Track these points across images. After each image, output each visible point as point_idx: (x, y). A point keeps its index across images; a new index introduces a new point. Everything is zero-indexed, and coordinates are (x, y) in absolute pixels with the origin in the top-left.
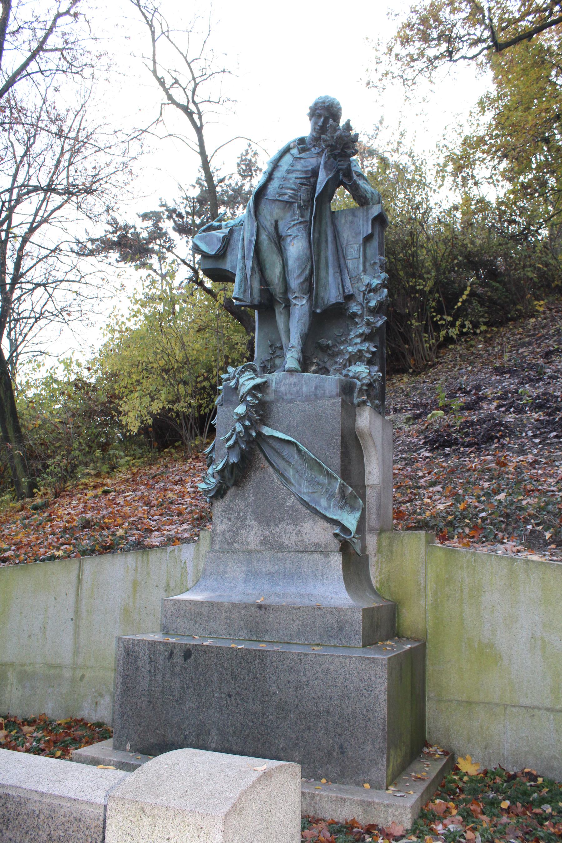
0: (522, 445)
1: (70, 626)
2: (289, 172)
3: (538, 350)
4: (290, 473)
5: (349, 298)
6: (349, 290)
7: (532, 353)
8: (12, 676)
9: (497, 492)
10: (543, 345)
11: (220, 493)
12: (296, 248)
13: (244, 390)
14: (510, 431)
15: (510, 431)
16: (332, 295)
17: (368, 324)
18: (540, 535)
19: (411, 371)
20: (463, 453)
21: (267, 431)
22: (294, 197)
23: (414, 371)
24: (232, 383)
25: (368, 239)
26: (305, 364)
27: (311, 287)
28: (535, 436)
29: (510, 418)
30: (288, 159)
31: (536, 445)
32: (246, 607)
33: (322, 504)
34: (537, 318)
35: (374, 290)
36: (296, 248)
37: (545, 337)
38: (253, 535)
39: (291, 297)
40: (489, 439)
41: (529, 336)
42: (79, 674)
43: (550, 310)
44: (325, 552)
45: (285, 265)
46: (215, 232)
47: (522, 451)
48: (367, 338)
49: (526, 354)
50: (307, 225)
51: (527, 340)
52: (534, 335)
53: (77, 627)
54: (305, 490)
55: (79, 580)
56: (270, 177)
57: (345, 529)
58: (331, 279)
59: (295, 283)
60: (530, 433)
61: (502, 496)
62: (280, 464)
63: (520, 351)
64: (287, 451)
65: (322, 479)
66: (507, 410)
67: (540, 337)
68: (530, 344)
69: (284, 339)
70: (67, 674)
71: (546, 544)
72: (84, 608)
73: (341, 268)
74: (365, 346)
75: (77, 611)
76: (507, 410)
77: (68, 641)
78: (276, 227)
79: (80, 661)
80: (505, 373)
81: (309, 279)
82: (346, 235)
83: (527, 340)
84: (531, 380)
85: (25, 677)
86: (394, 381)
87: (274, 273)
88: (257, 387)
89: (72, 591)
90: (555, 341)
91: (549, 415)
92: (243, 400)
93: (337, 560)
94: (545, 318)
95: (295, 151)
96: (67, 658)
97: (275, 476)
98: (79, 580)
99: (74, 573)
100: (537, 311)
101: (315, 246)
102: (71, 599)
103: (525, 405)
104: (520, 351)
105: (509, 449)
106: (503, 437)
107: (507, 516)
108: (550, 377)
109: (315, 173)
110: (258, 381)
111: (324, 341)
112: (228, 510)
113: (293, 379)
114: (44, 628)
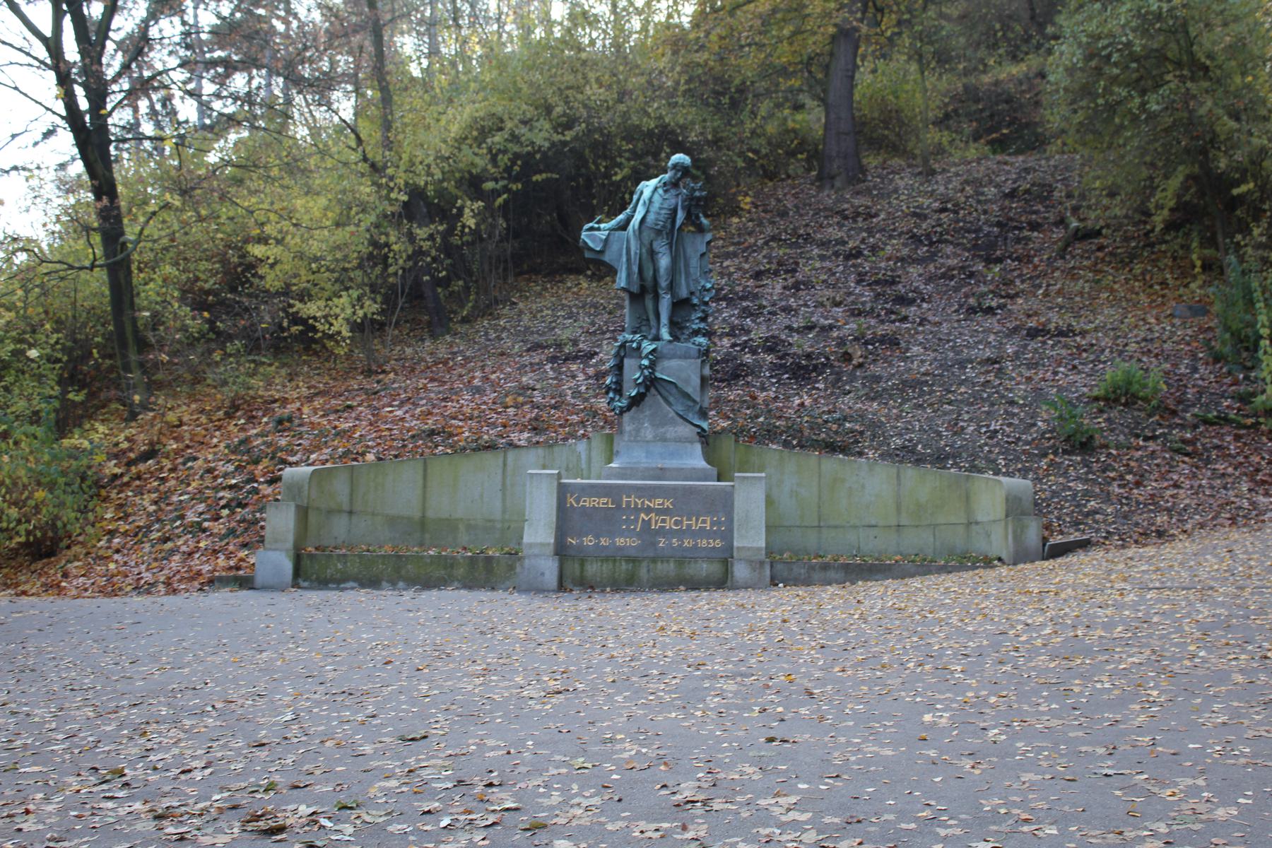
0: (763, 383)
1: (500, 494)
2: (661, 209)
3: (747, 266)
4: (671, 399)
5: (692, 293)
6: (693, 289)
7: (740, 269)
8: (461, 527)
9: (757, 417)
10: (751, 259)
11: (629, 408)
12: (664, 261)
13: (645, 352)
14: (752, 371)
15: (752, 371)
16: (684, 293)
17: (703, 311)
18: (790, 442)
19: (589, 273)
20: (719, 388)
21: (658, 375)
22: (664, 227)
23: (593, 274)
24: (634, 345)
25: (703, 255)
26: (676, 338)
27: (672, 287)
28: (771, 377)
29: (748, 358)
30: (656, 197)
31: (773, 384)
32: (653, 469)
33: (690, 417)
34: (740, 217)
35: (708, 290)
36: (664, 261)
37: (753, 248)
38: (648, 432)
39: (661, 292)
40: (736, 377)
41: (734, 244)
42: (506, 525)
43: (756, 207)
44: (691, 442)
45: (656, 270)
46: (596, 233)
47: (763, 389)
48: (703, 319)
49: (732, 270)
50: (670, 244)
51: (731, 249)
52: (739, 243)
53: (504, 495)
54: (680, 408)
55: (505, 464)
56: (647, 212)
57: (703, 430)
58: (683, 282)
59: (663, 283)
60: (768, 374)
61: (761, 419)
62: (666, 394)
63: (725, 264)
64: (669, 387)
65: (691, 404)
66: (742, 350)
67: (747, 248)
68: (735, 255)
69: (652, 317)
70: (499, 526)
71: (794, 447)
72: (508, 482)
73: (688, 274)
74: (702, 325)
75: (504, 484)
76: (742, 350)
77: (498, 504)
78: (651, 244)
79: (507, 517)
80: (721, 300)
81: (671, 282)
82: (689, 250)
83: (731, 249)
84: (752, 315)
85: (470, 528)
86: (569, 284)
87: (649, 274)
88: (654, 350)
89: (500, 471)
90: (764, 257)
91: (781, 358)
92: (646, 357)
93: (698, 447)
94: (751, 220)
95: (660, 191)
96: (498, 516)
97: (662, 401)
98: (505, 464)
99: (501, 460)
100: (742, 209)
101: (674, 260)
102: (499, 477)
103: (758, 346)
104: (725, 264)
105: (754, 386)
106: (747, 375)
107: (768, 431)
108: (770, 313)
109: (674, 211)
110: (654, 346)
111: (675, 319)
112: (632, 418)
113: (671, 346)
114: (481, 496)
